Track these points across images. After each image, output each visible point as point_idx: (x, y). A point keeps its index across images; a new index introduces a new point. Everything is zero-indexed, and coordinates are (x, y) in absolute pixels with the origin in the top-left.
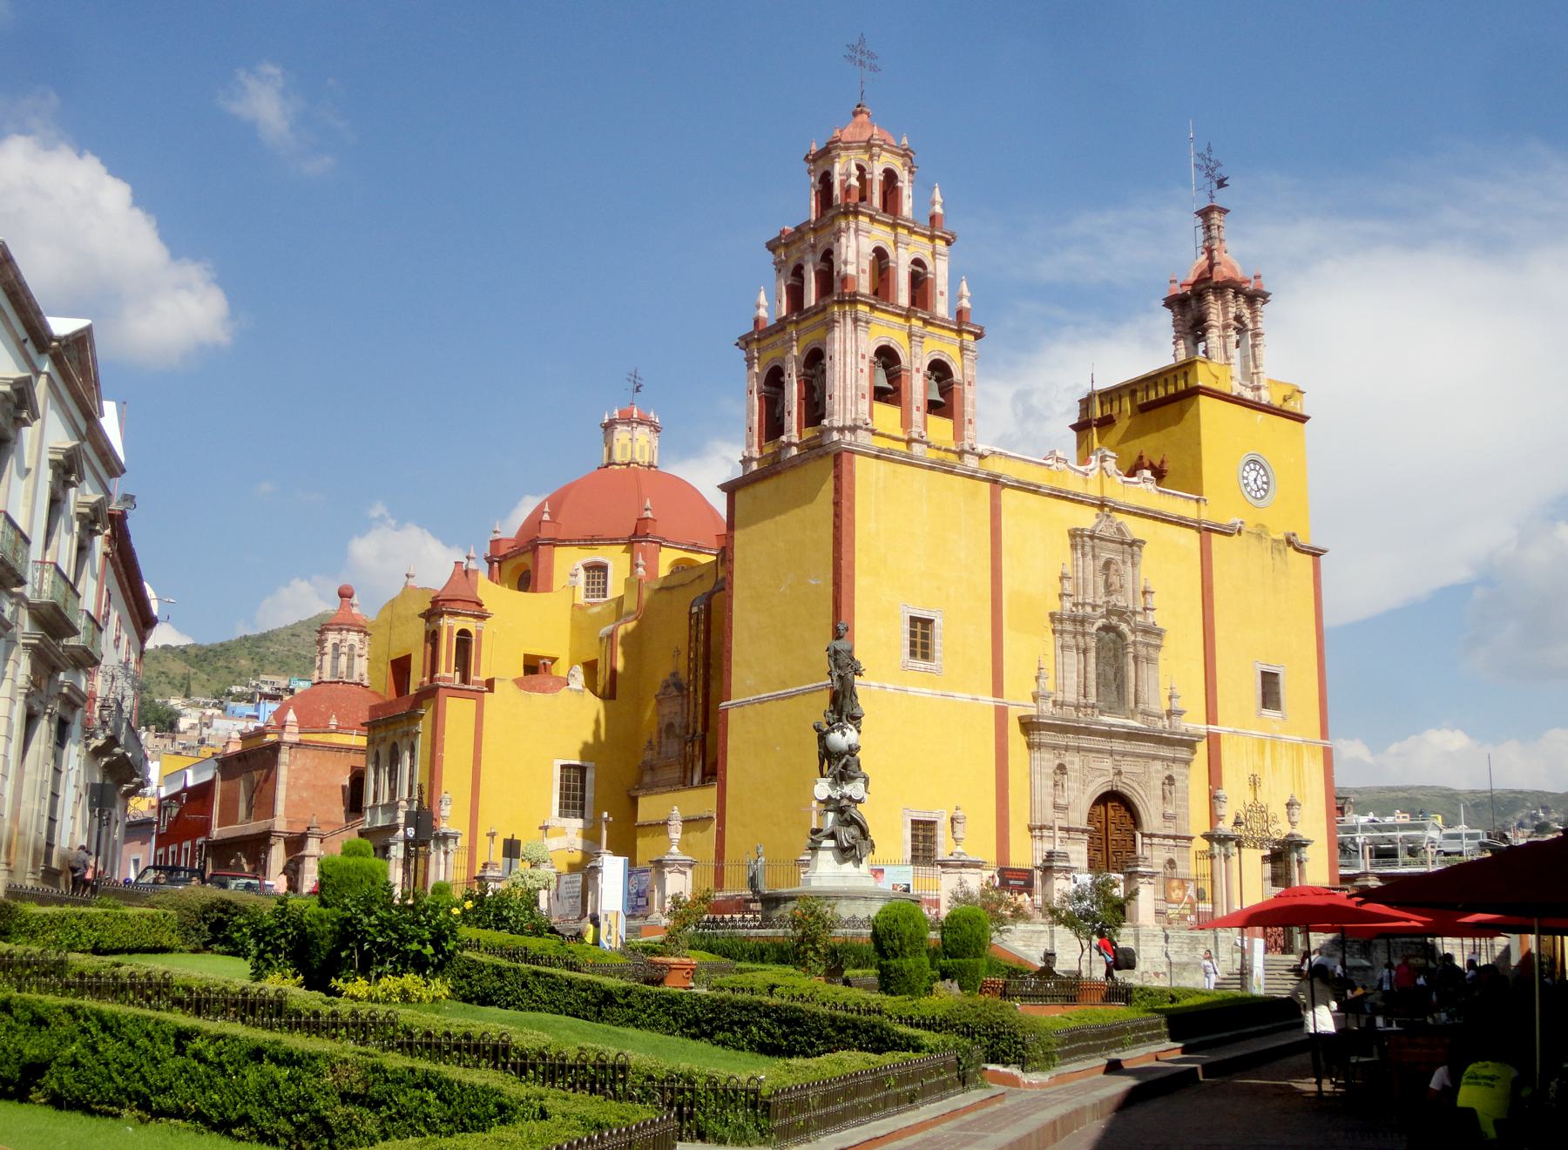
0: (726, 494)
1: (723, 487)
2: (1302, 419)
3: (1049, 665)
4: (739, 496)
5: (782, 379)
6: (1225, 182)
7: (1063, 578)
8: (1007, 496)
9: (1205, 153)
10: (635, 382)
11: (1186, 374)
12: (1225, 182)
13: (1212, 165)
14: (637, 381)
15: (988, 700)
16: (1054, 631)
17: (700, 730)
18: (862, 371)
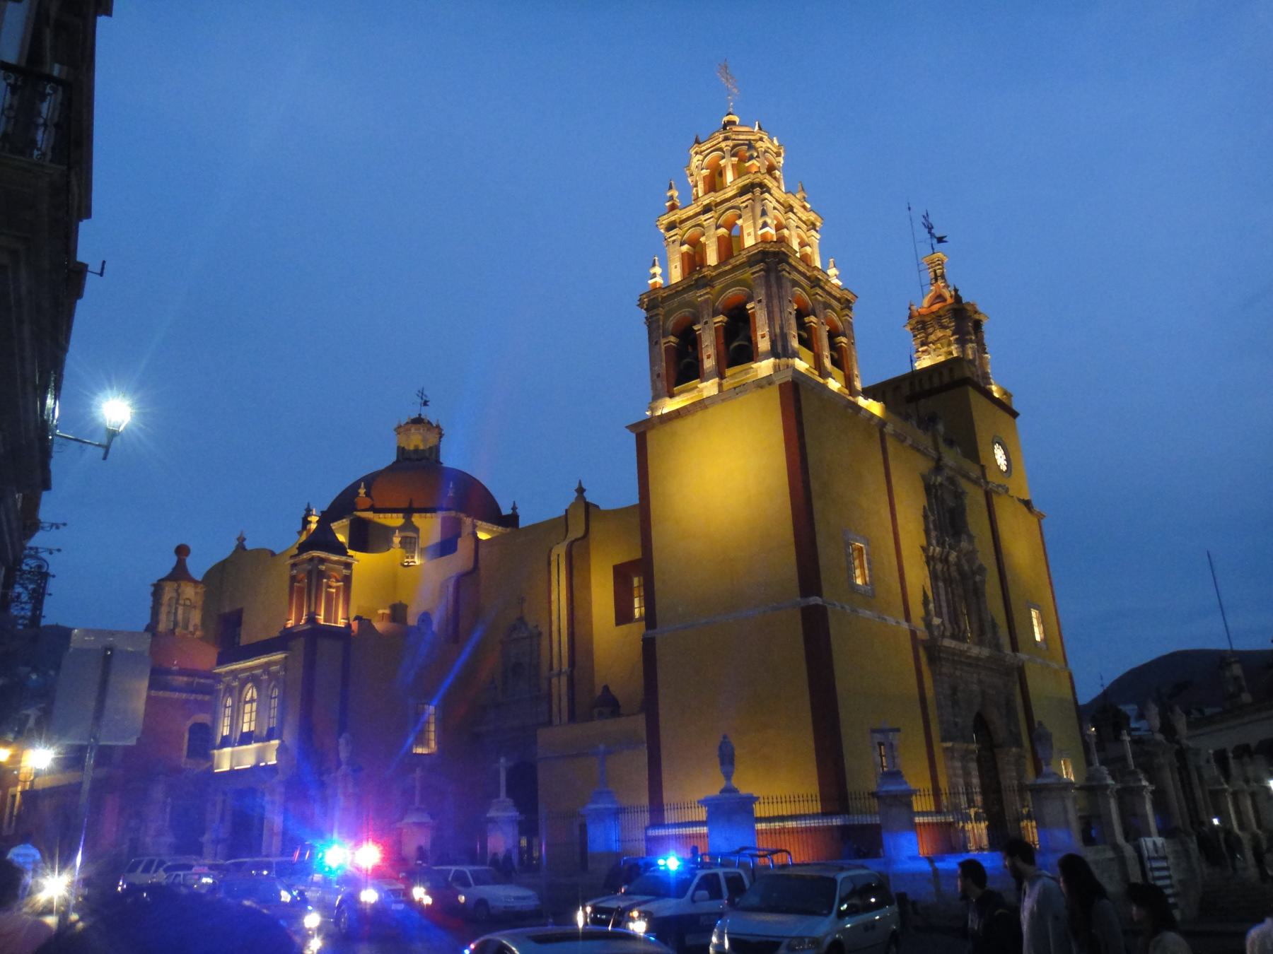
0: (633, 436)
1: (632, 427)
2: (1014, 414)
3: (930, 594)
4: (651, 437)
5: (696, 328)
6: (945, 239)
7: (925, 517)
8: (891, 445)
9: (926, 215)
10: (422, 399)
11: (951, 370)
12: (945, 239)
13: (930, 226)
14: (424, 398)
15: (905, 625)
16: (928, 563)
17: (565, 667)
18: (790, 313)
